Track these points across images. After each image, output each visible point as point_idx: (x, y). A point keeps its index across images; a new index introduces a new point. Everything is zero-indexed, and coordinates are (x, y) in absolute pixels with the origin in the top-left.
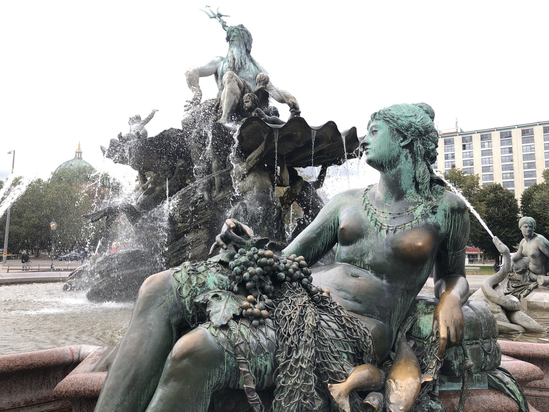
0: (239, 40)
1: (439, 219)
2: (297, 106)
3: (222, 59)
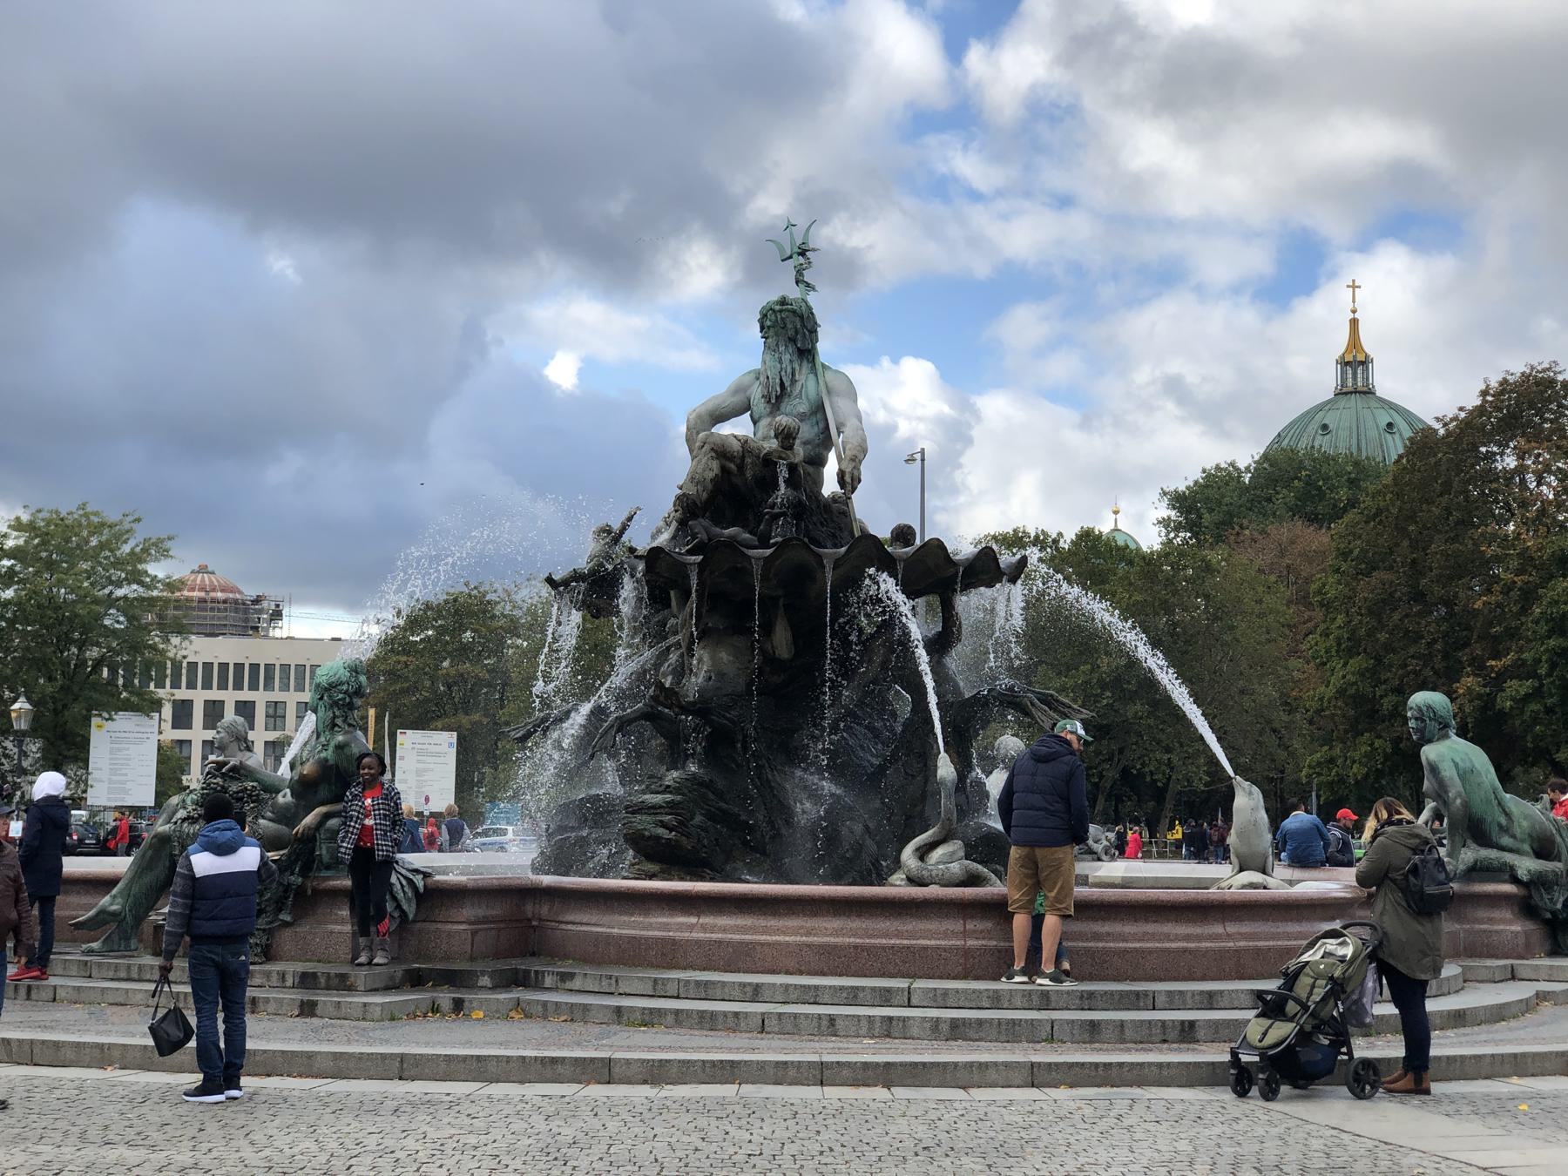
0: (776, 334)
1: (328, 754)
2: (848, 479)
3: (757, 375)
